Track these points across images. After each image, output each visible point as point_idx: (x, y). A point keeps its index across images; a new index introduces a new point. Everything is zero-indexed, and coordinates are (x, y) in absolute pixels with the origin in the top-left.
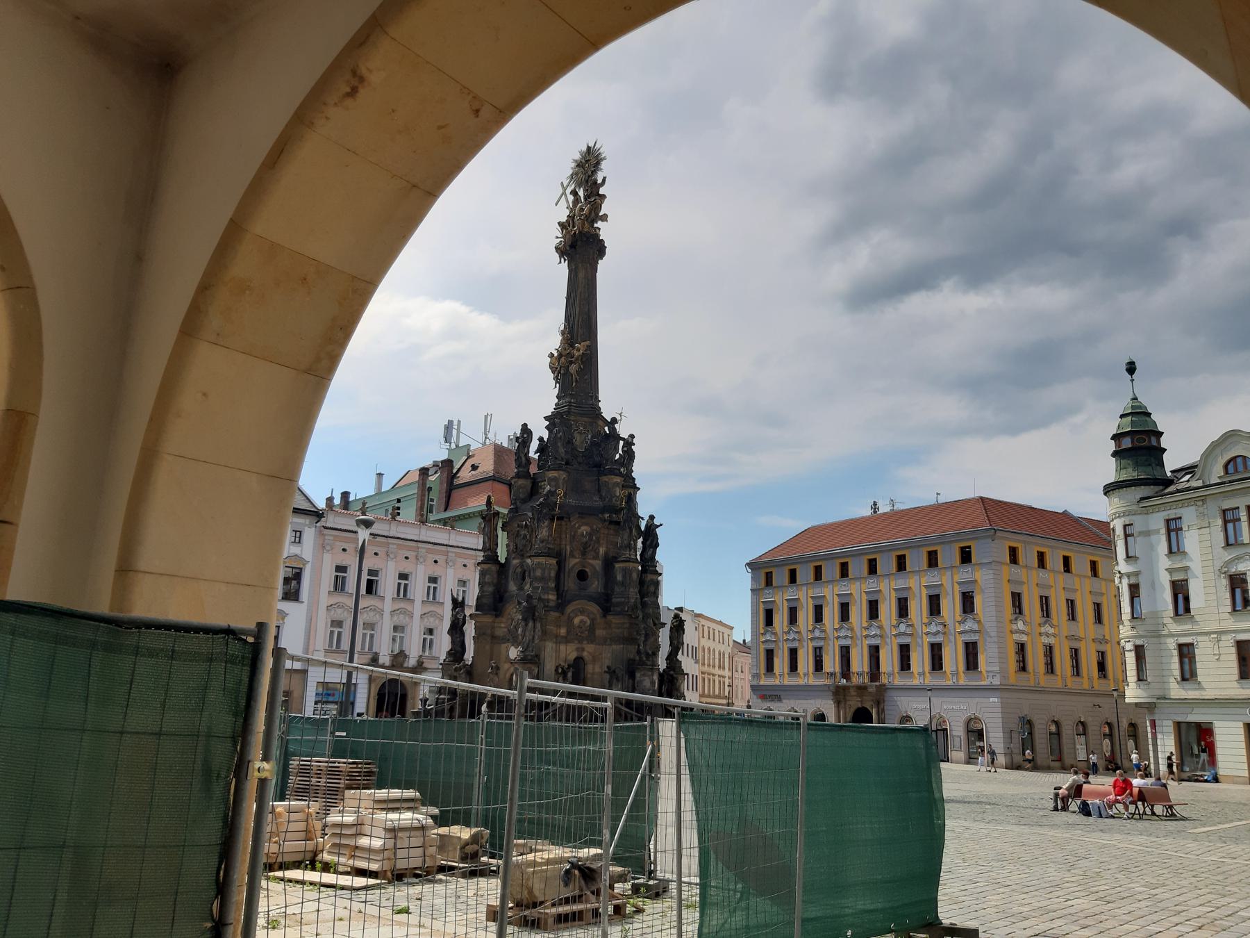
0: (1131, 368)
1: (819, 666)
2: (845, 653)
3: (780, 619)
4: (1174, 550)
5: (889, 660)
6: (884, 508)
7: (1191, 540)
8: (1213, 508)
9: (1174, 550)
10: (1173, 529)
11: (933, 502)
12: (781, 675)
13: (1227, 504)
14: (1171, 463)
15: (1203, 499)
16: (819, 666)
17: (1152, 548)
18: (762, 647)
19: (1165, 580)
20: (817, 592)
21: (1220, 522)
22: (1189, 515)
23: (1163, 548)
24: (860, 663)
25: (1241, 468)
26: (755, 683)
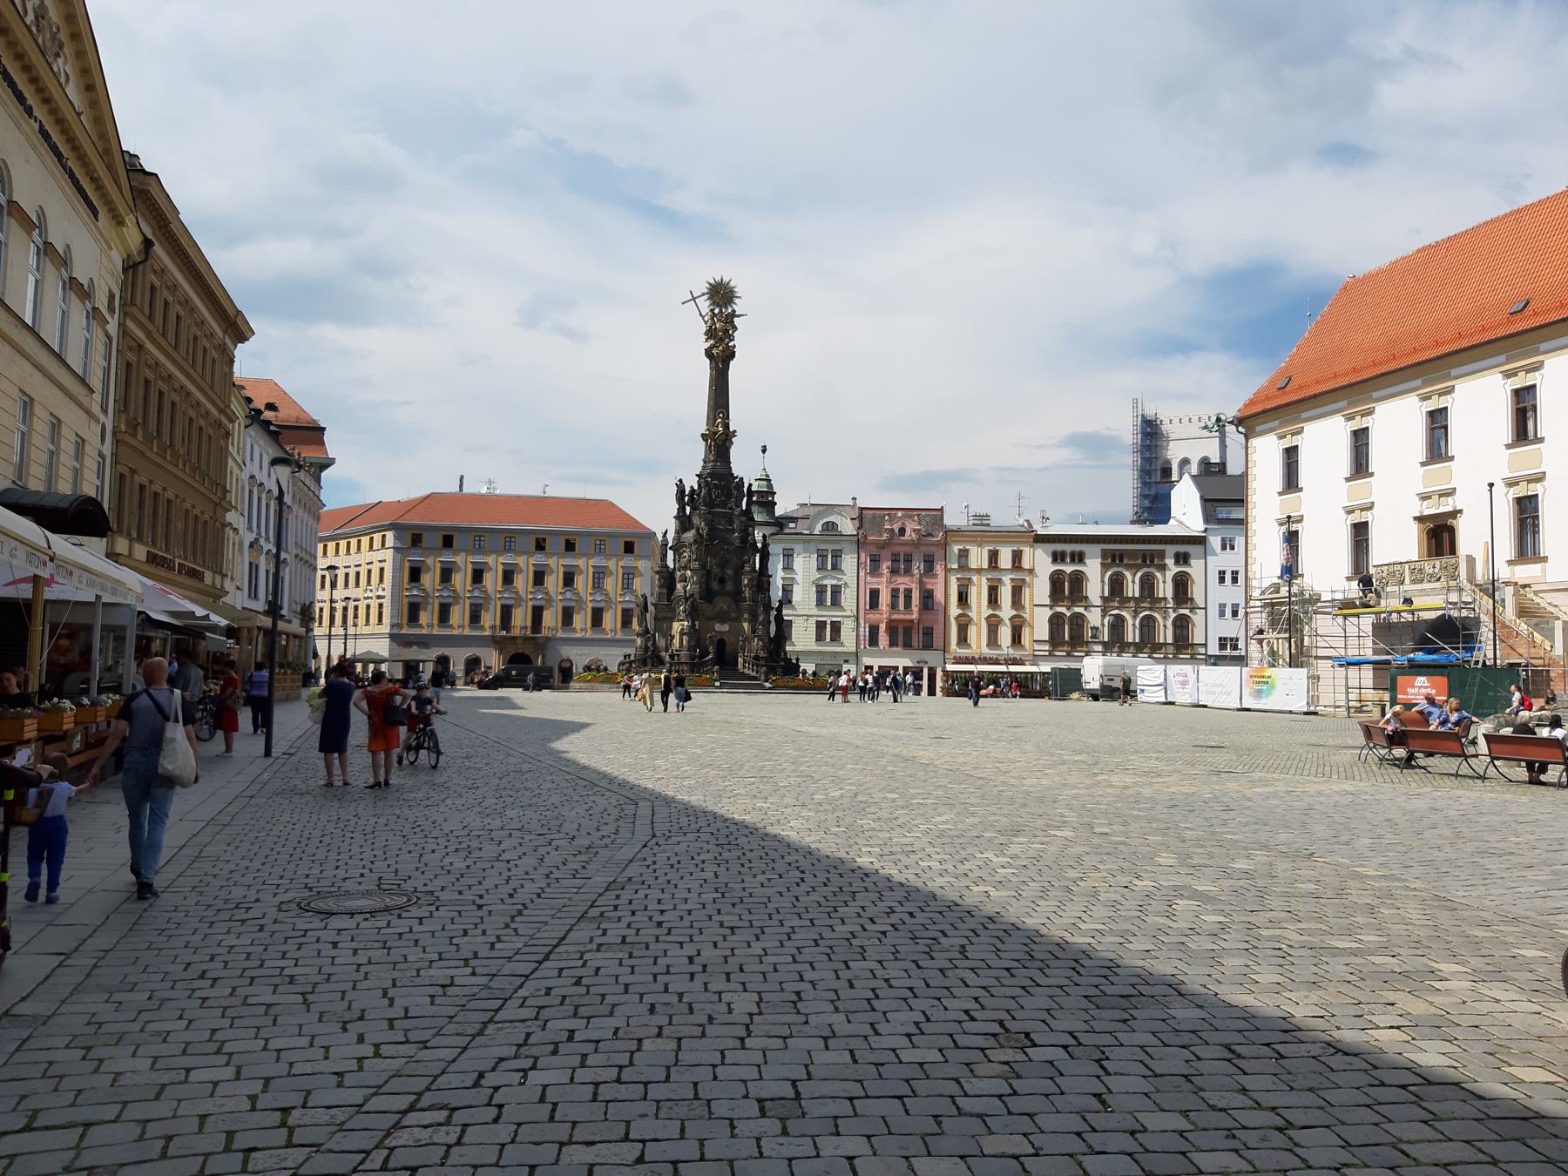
0: (764, 451)
1: (475, 618)
2: (506, 612)
3: (430, 580)
4: (788, 567)
5: (550, 618)
6: (475, 487)
7: (799, 562)
8: (813, 547)
9: (788, 567)
10: (788, 555)
11: (538, 492)
12: (430, 626)
13: (822, 547)
14: (779, 511)
16: (475, 618)
17: (775, 565)
18: (406, 601)
19: (779, 583)
20: (478, 559)
22: (798, 548)
23: (780, 566)
24: (521, 619)
26: (395, 631)
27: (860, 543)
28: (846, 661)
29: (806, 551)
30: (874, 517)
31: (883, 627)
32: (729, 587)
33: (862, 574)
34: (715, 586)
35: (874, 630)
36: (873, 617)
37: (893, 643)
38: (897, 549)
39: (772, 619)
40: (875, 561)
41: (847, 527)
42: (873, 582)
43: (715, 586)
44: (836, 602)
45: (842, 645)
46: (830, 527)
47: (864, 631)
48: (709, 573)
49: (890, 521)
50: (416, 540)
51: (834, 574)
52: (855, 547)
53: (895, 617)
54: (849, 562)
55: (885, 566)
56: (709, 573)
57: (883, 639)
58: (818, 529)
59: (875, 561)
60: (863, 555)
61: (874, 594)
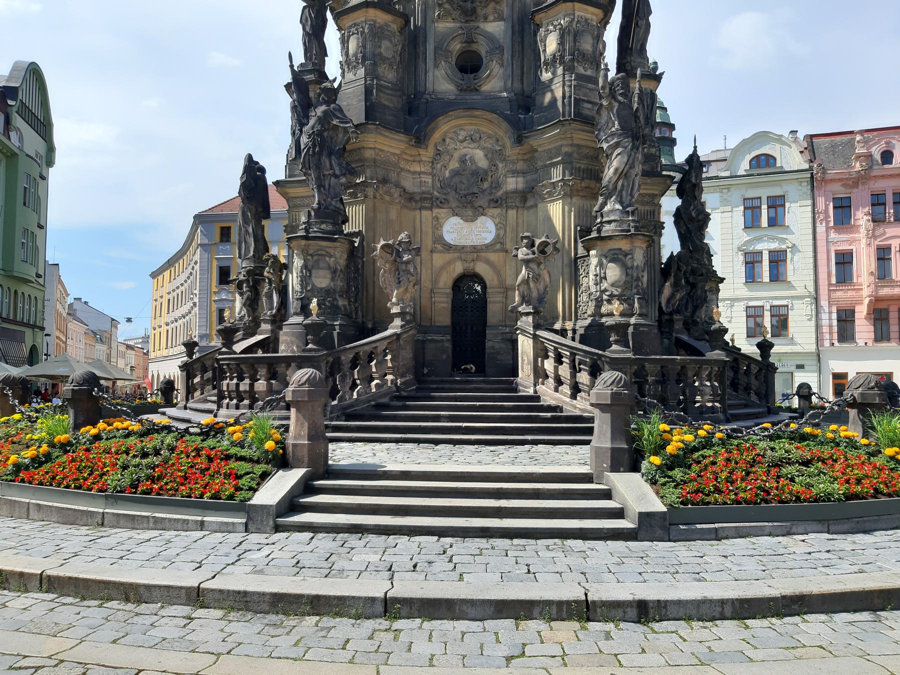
13: (751, 194)
15: (728, 188)
21: (742, 208)
25: (763, 163)
27: (814, 181)
28: (800, 367)
29: (724, 202)
30: (834, 146)
31: (861, 311)
32: (495, 81)
33: (821, 229)
34: (440, 81)
35: (846, 319)
36: (844, 295)
37: (881, 336)
38: (879, 186)
39: (668, 220)
40: (843, 208)
41: (792, 159)
42: (841, 241)
43: (440, 81)
44: (777, 276)
45: (792, 342)
46: (763, 163)
47: (829, 319)
48: (414, 42)
49: (866, 142)
50: (225, 234)
51: (773, 232)
52: (806, 188)
53: (885, 292)
54: (798, 214)
55: (862, 217)
56: (414, 42)
57: (863, 329)
58: (744, 166)
59: (843, 208)
60: (821, 202)
61: (844, 260)
